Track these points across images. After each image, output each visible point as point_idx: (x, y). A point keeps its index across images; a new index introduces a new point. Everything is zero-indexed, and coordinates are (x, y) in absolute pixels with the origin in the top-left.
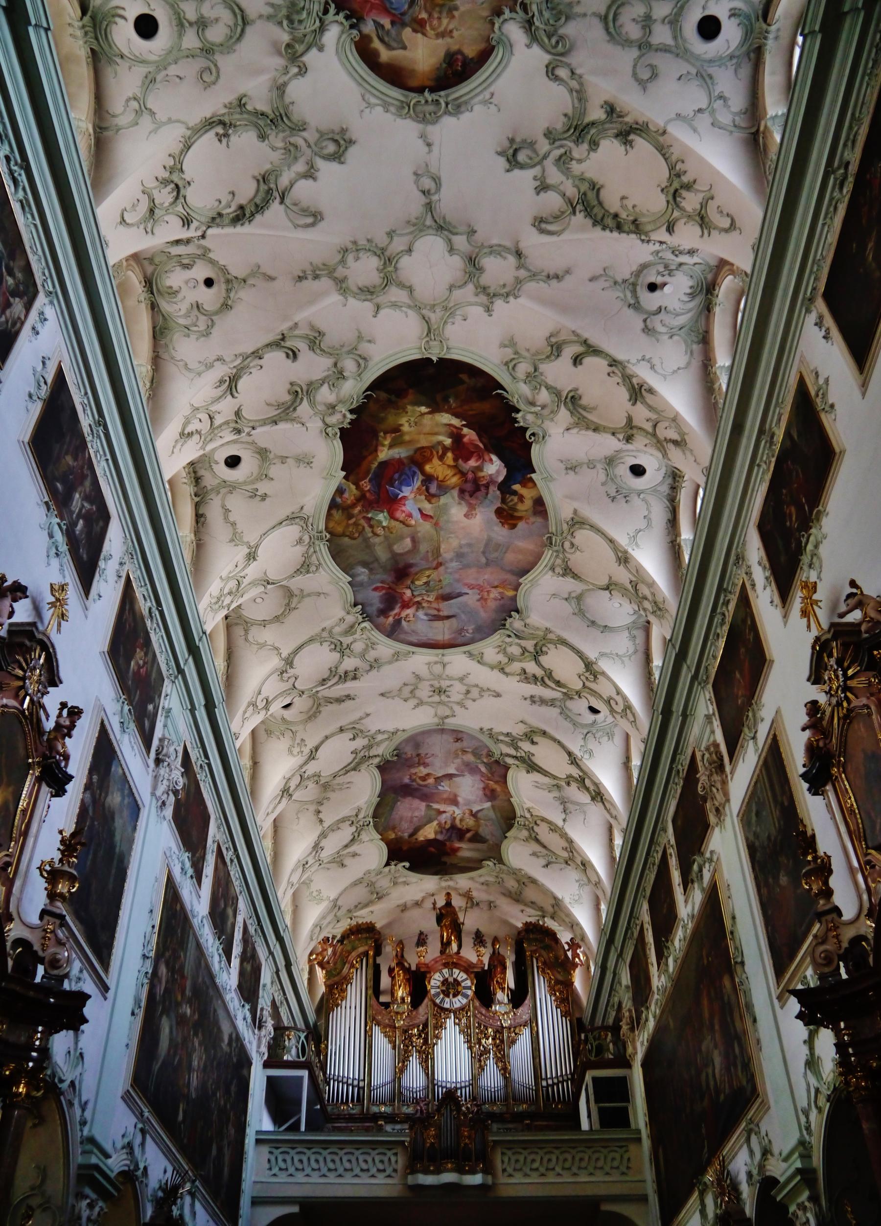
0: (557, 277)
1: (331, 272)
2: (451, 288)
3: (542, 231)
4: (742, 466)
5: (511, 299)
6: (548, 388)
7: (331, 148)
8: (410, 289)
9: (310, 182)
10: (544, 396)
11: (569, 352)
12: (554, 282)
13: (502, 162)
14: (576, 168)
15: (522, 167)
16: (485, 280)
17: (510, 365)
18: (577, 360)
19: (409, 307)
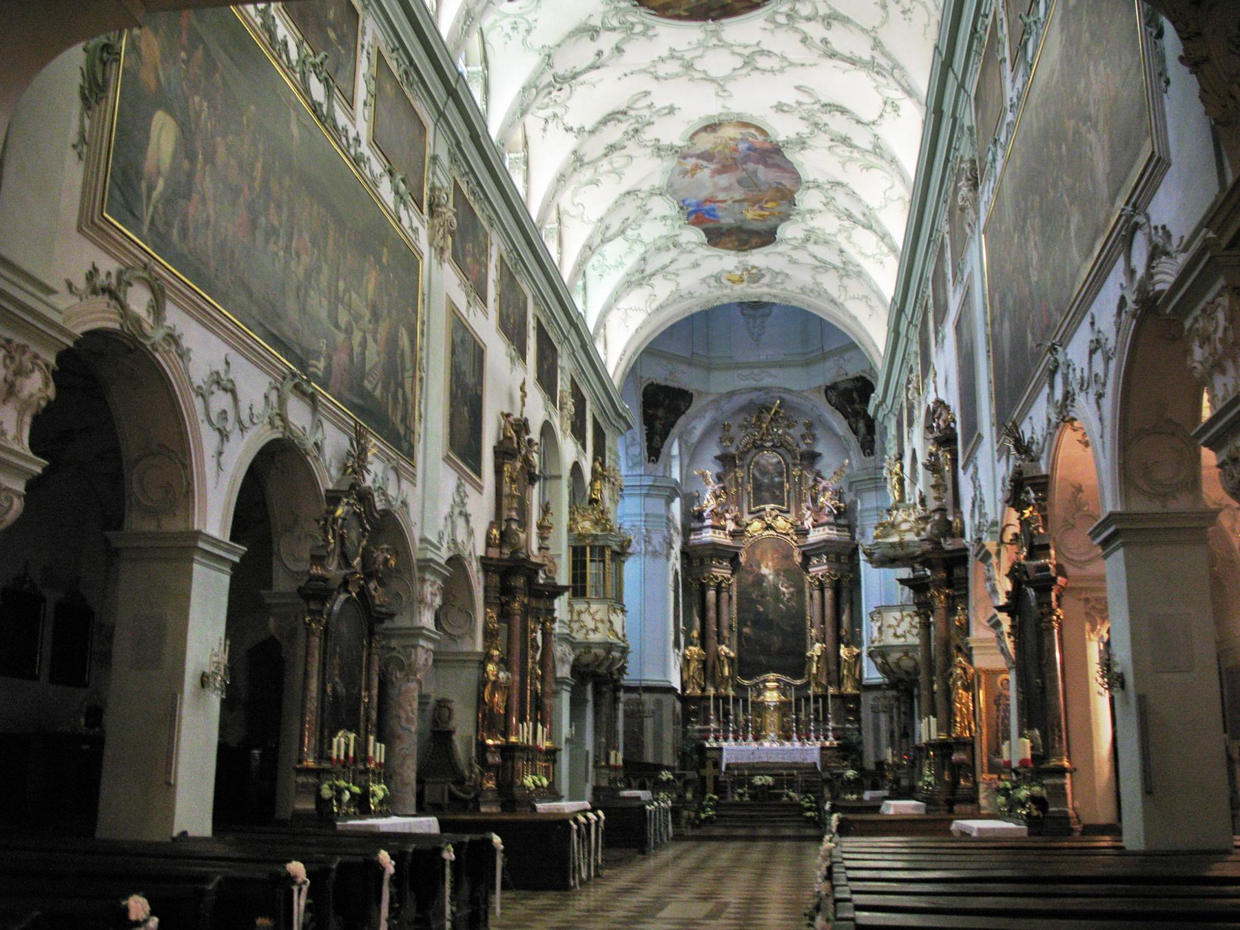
0: (626, 75)
1: (791, 64)
2: (701, 57)
3: (645, 92)
4: (516, 236)
5: (656, 59)
6: (614, 29)
7: (785, 108)
8: (733, 53)
9: (800, 100)
10: (615, 23)
11: (606, 54)
12: (627, 72)
13: (676, 106)
14: (632, 121)
15: (664, 108)
16: (680, 62)
17: (647, 28)
18: (599, 54)
19: (732, 45)
